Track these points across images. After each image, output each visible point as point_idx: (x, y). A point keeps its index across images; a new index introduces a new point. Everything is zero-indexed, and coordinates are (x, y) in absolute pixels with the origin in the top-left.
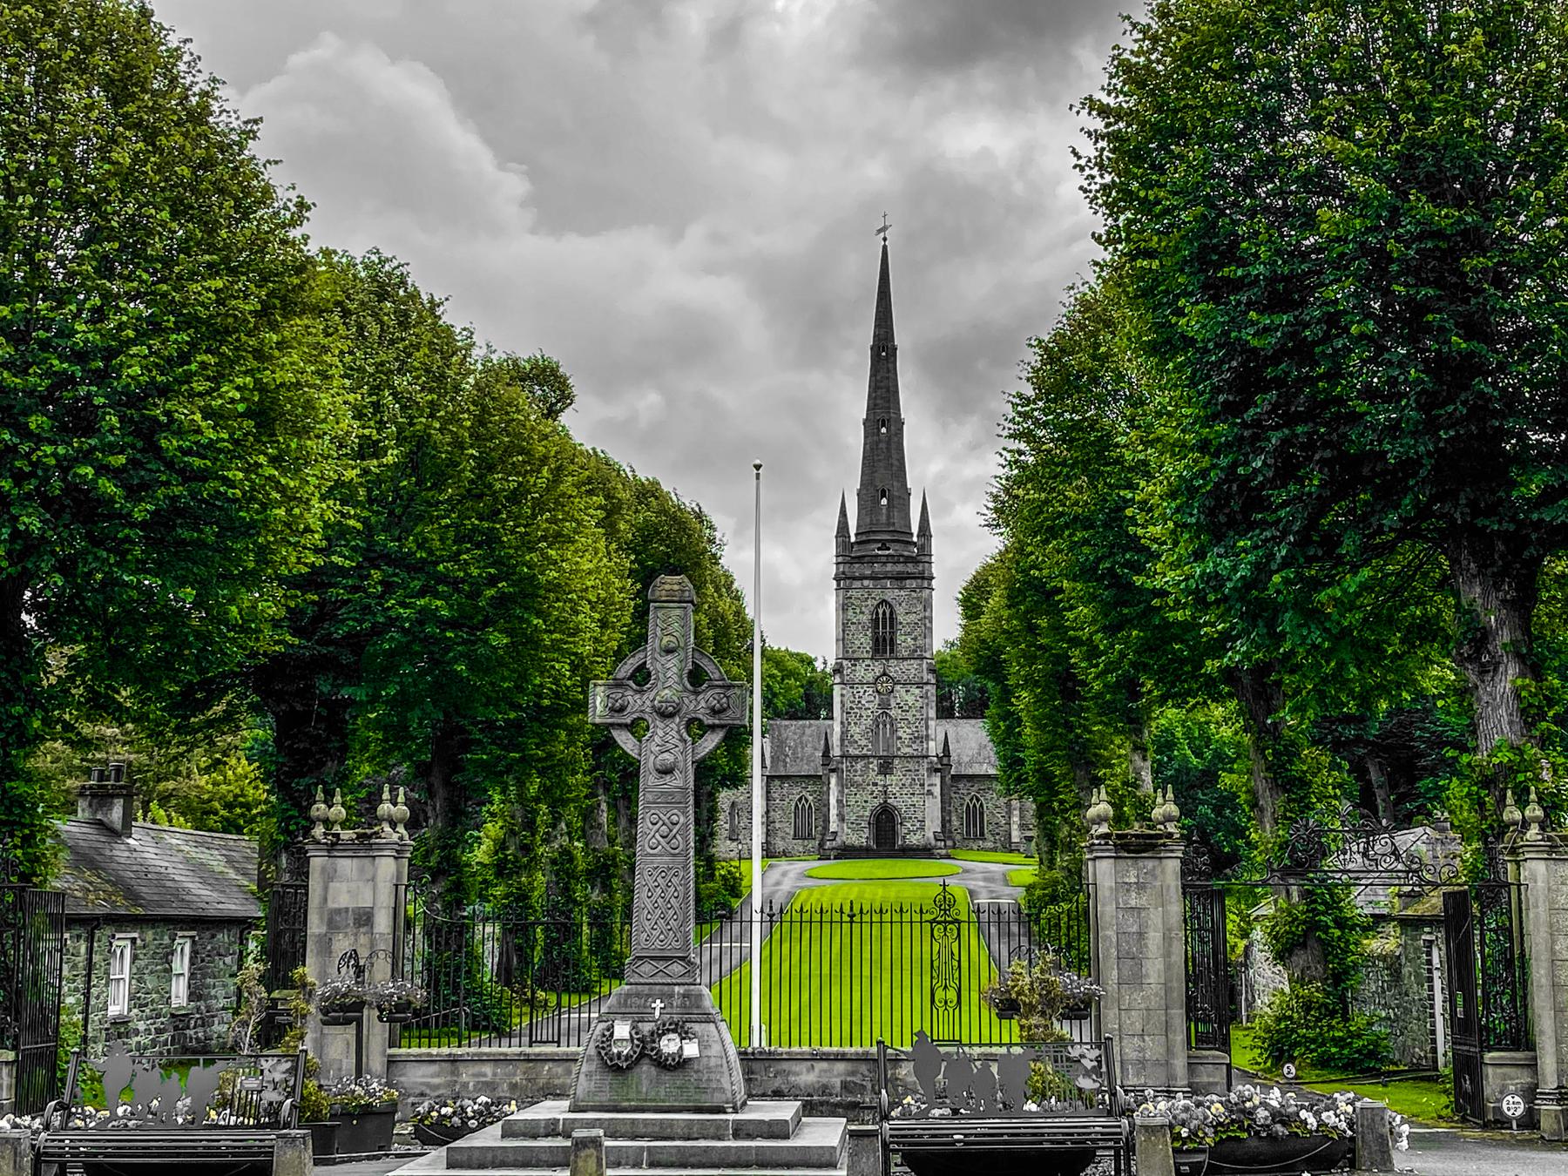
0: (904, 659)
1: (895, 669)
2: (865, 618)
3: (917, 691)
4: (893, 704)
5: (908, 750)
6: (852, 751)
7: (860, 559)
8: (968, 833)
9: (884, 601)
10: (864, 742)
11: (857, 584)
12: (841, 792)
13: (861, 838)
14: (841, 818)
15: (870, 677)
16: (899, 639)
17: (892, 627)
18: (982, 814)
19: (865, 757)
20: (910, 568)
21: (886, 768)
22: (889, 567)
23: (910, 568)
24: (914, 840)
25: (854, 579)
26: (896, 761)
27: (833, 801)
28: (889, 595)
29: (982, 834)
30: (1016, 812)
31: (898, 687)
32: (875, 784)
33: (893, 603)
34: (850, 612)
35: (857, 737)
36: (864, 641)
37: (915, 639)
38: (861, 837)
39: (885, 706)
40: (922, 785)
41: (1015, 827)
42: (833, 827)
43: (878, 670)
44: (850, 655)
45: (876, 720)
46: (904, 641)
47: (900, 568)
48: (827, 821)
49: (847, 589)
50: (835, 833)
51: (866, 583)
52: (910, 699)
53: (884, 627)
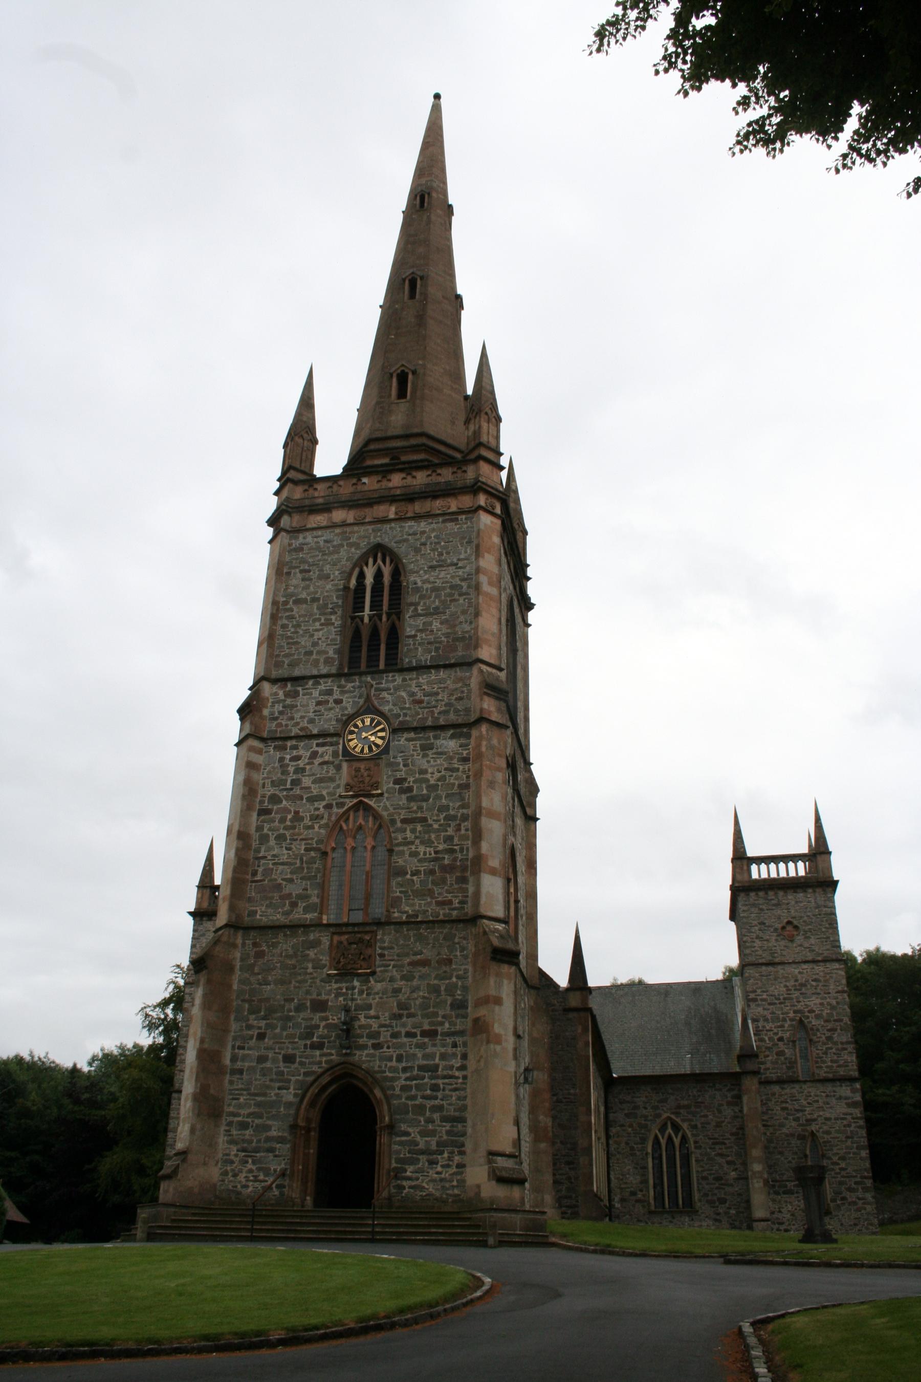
1: (396, 692)
2: (330, 590)
3: (450, 745)
4: (387, 784)
6: (264, 914)
8: (659, 1197)
9: (379, 551)
10: (295, 890)
15: (329, 721)
16: (410, 625)
18: (686, 1159)
19: (294, 927)
21: (355, 948)
22: (397, 480)
23: (446, 475)
24: (425, 1181)
25: (314, 509)
28: (389, 535)
29: (689, 1200)
30: (756, 1152)
31: (402, 740)
32: (320, 1006)
33: (401, 550)
34: (296, 580)
35: (280, 874)
36: (325, 639)
37: (450, 623)
40: (459, 1006)
41: (757, 1185)
44: (283, 672)
45: (336, 828)
46: (420, 631)
47: (421, 478)
49: (295, 532)
51: (339, 515)
52: (433, 768)
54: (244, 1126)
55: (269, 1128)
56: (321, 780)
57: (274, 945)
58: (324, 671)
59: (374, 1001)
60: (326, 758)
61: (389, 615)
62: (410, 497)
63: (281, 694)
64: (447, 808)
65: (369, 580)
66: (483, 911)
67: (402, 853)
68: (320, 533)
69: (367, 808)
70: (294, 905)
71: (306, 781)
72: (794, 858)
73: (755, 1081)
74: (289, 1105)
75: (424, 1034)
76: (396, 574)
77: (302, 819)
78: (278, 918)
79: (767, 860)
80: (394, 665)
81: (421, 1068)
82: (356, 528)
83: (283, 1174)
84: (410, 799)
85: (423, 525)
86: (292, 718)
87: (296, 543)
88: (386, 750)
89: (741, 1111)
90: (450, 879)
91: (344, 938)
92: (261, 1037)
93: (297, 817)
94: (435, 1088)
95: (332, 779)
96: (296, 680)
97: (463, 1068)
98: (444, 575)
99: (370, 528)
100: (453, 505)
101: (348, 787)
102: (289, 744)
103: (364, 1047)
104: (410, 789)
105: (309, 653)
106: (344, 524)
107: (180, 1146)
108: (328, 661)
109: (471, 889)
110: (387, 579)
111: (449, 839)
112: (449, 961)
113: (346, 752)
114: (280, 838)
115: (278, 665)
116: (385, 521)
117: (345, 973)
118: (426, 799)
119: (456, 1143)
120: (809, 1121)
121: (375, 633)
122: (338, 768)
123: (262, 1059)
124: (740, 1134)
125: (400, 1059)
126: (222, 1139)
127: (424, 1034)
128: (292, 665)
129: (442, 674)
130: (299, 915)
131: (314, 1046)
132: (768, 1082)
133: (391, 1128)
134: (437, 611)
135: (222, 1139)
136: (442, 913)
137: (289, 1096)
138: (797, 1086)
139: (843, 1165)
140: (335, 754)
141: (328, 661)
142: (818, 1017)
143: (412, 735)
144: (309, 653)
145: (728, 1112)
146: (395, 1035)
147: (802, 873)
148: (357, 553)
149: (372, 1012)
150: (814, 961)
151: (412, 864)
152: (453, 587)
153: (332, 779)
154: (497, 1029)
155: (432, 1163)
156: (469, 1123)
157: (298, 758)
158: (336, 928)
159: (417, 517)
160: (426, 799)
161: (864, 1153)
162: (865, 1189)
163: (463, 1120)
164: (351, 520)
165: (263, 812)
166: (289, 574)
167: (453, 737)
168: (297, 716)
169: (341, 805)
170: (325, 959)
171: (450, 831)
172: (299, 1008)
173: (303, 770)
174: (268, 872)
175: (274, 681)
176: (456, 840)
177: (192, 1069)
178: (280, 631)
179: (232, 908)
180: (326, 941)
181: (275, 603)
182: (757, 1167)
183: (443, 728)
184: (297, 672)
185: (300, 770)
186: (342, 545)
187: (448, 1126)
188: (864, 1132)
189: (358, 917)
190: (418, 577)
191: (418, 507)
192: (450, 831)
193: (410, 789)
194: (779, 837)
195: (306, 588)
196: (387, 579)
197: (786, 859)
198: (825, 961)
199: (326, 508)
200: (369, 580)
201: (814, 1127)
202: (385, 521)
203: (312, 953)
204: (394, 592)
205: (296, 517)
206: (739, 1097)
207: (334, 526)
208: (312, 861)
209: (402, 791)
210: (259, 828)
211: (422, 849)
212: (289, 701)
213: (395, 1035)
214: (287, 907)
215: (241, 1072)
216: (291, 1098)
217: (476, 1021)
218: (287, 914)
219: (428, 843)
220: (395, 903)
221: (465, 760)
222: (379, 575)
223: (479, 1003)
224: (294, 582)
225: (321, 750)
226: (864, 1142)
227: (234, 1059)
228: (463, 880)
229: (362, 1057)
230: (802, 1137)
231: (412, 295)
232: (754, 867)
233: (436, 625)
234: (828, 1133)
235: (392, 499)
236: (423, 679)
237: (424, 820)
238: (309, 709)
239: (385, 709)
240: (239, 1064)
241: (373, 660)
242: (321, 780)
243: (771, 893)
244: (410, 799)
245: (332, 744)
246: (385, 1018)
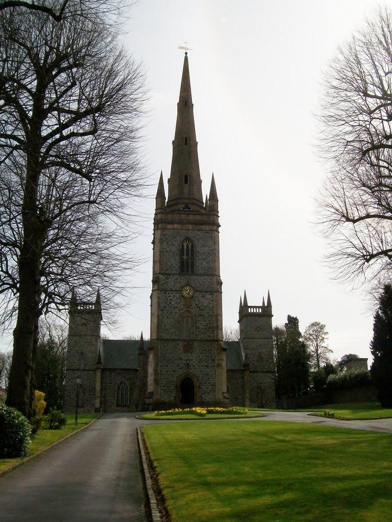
0: (201, 275)
2: (175, 249)
3: (209, 297)
5: (203, 336)
6: (164, 336)
7: (173, 212)
11: (170, 226)
12: (156, 365)
13: (170, 397)
14: (156, 382)
15: (178, 286)
17: (192, 255)
19: (174, 340)
20: (204, 218)
21: (188, 346)
22: (191, 217)
26: (196, 344)
27: (150, 370)
31: (197, 294)
32: (181, 359)
36: (175, 262)
37: (208, 263)
38: (170, 397)
39: (188, 306)
40: (213, 360)
42: (151, 388)
43: (183, 282)
46: (201, 264)
47: (198, 218)
48: (145, 385)
50: (152, 393)
51: (176, 226)
53: (187, 255)
54: (164, 386)
55: (170, 387)
56: (177, 303)
57: (168, 344)
58: (175, 272)
59: (194, 358)
60: (178, 297)
61: (191, 259)
62: (196, 223)
63: (164, 278)
64: (208, 313)
65: (185, 248)
66: (219, 339)
67: (198, 324)
68: (170, 231)
69: (189, 311)
70: (172, 334)
71: (173, 303)
72: (259, 307)
73: (248, 372)
74: (175, 382)
75: (206, 366)
76: (192, 246)
77: (172, 313)
78: (168, 337)
79: (253, 307)
80: (193, 273)
81: (206, 374)
82: (181, 231)
83: (175, 397)
84: (200, 310)
85: (199, 233)
86: (167, 285)
87: (164, 233)
88: (193, 297)
89: (244, 380)
90: (211, 330)
91: (185, 343)
92: (167, 366)
93: (171, 313)
94: (209, 378)
95: (179, 303)
96: (169, 275)
97: (215, 374)
98: (206, 249)
99: (185, 231)
100: (207, 227)
101: (184, 305)
102: (167, 292)
103: (192, 369)
104: (200, 307)
105: (171, 267)
106: (177, 229)
107: (149, 391)
108: (176, 270)
109: (215, 333)
110: (190, 248)
111: (209, 321)
112: (211, 350)
113: (183, 296)
114: (167, 317)
115: (162, 270)
116: (188, 230)
117: (186, 351)
118: (203, 310)
119: (214, 391)
120: (260, 383)
121: (187, 262)
122: (181, 300)
123: (167, 371)
124: (243, 387)
125: (200, 372)
126: (159, 389)
127: (206, 366)
128: (167, 270)
129: (206, 277)
130: (173, 337)
131: (180, 368)
132: (250, 372)
133: (199, 387)
134: (204, 259)
135: (159, 389)
136: (209, 338)
137: (175, 379)
138: (257, 374)
139: (268, 395)
140: (180, 296)
141: (176, 270)
142: (265, 354)
143: (200, 293)
144: (171, 267)
145: (240, 380)
146: (199, 366)
147: (260, 311)
148: (182, 239)
149: (194, 361)
150: (265, 338)
151: (201, 326)
152: (209, 253)
153: (179, 303)
154: (223, 366)
155: (209, 395)
156: (217, 386)
157: (170, 296)
158: (184, 340)
159: (198, 230)
160: (203, 310)
161: (274, 392)
162: (274, 402)
163: (215, 385)
164: (179, 228)
165: (161, 310)
166: (163, 242)
167: (209, 295)
168: (169, 284)
169: (182, 310)
170: (181, 348)
171: (210, 319)
172: (176, 360)
173: (172, 300)
174: (165, 326)
175: (162, 274)
176: (211, 321)
177: (151, 375)
178: (162, 260)
179: (157, 335)
180: (181, 344)
181: (160, 251)
182: (248, 395)
183: (207, 292)
184: (168, 272)
185: (170, 300)
186: (177, 236)
187: (212, 387)
188: (274, 387)
189: (188, 338)
190: (199, 249)
191: (198, 227)
192: (210, 319)
193: (200, 307)
194: (255, 301)
195: (168, 247)
196: (190, 248)
197: (256, 307)
198: (268, 338)
199: (172, 223)
200: (185, 248)
201: (261, 385)
202: (188, 230)
203: (178, 347)
204: (192, 251)
205: (164, 225)
206: (243, 376)
207: (175, 229)
208: (176, 324)
209: (198, 307)
210: (162, 315)
211: (203, 322)
212: (166, 280)
213: (199, 366)
214: (170, 335)
215: (162, 374)
216: (175, 380)
217: (218, 364)
218: (170, 337)
219: (205, 321)
220: (197, 335)
221: (213, 301)
222: (187, 245)
223: (219, 360)
224: (164, 245)
225: (176, 295)
226: (274, 389)
227: (161, 371)
228: (213, 331)
229: (191, 371)
230: (258, 388)
231: (186, 144)
232: (249, 309)
233: (204, 263)
234: (265, 386)
235: (191, 224)
236: (202, 278)
237: (203, 315)
238: (171, 283)
239: (192, 285)
240: (162, 373)
241: (188, 271)
242: (177, 303)
243: (254, 317)
244: (200, 310)
245: (179, 293)
246: (196, 362)
